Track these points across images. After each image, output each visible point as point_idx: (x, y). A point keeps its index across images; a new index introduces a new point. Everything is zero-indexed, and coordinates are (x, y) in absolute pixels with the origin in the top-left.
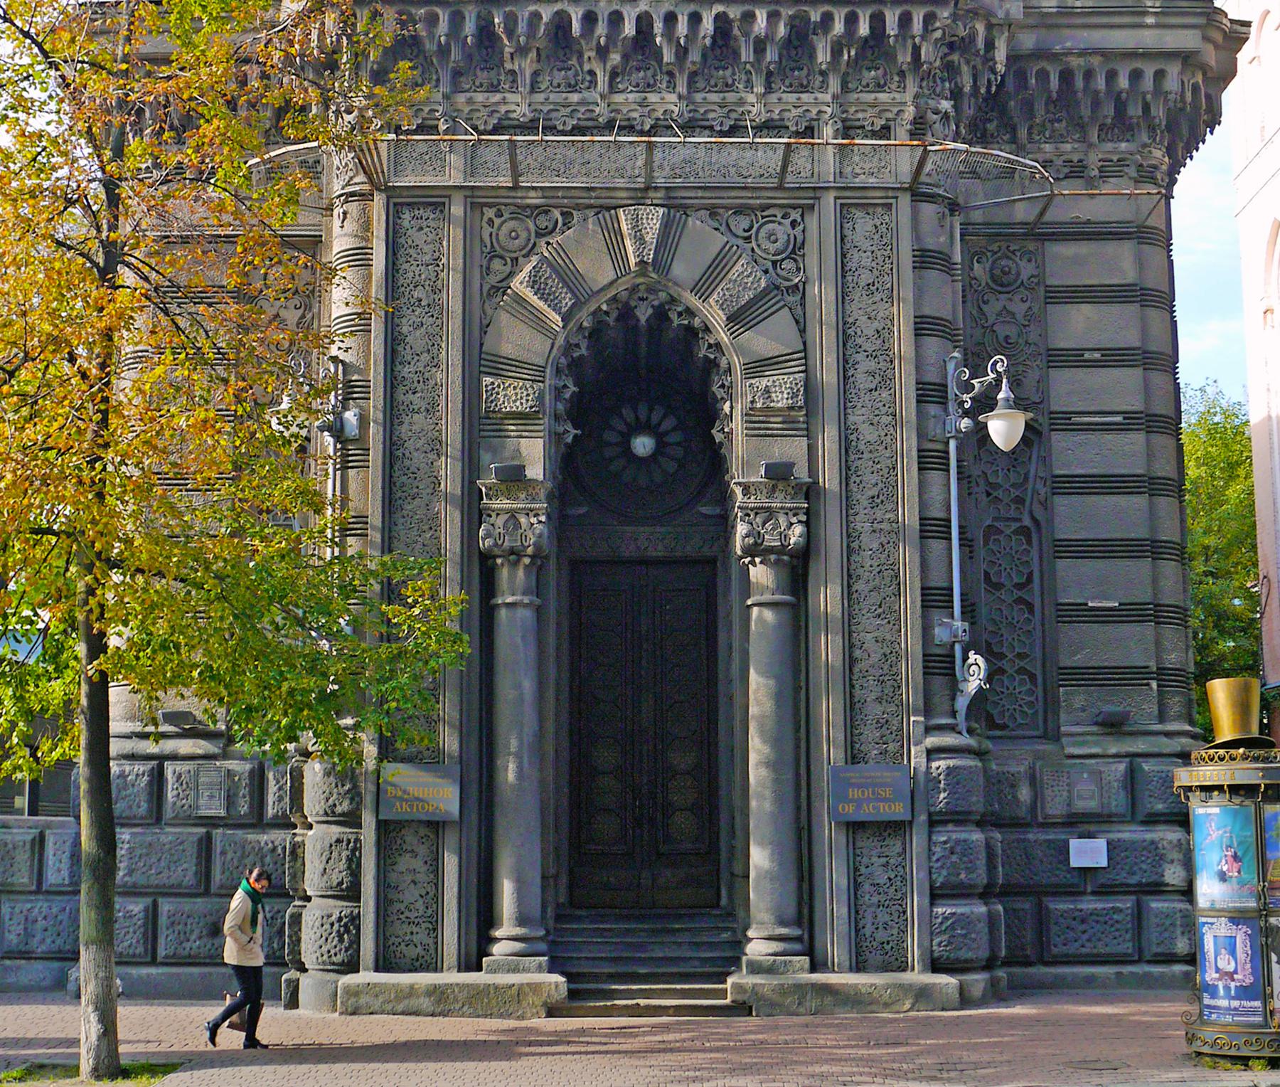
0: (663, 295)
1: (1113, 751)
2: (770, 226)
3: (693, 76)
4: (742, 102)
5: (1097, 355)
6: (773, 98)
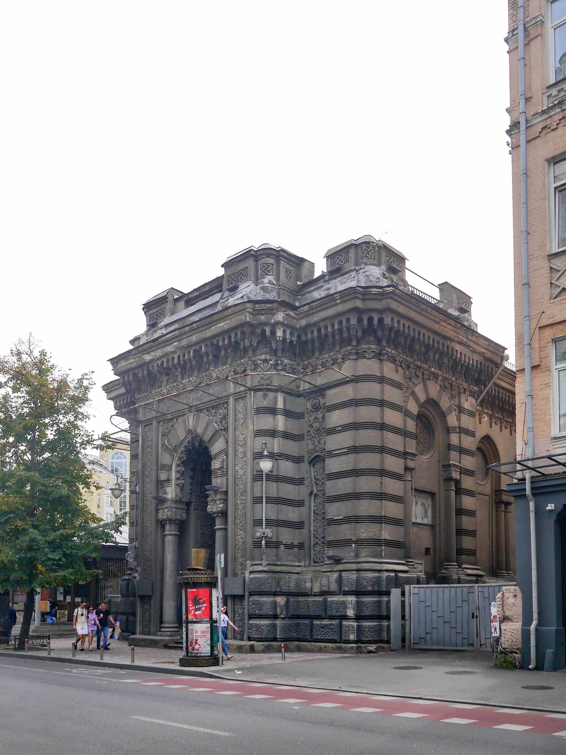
6: (216, 370)
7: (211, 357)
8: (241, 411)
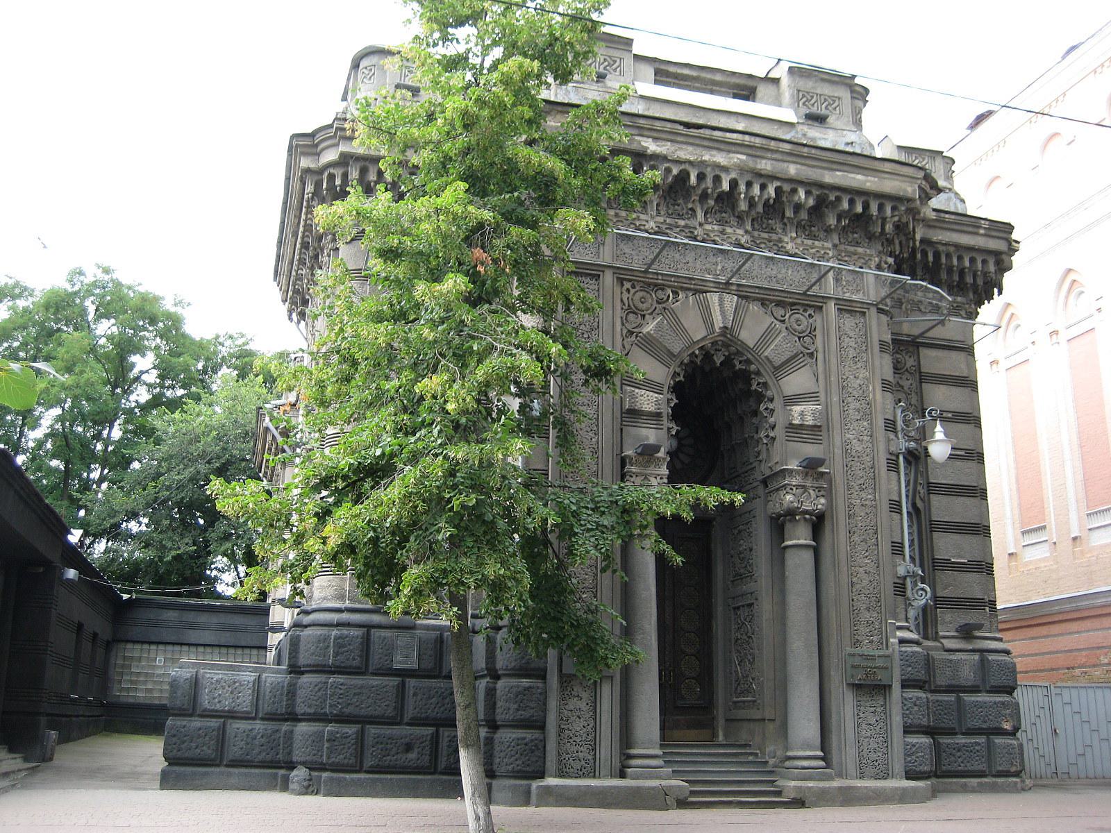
1: (971, 647)
2: (797, 315)
3: (753, 220)
4: (780, 241)
5: (950, 415)
6: (799, 241)
7: (804, 215)
8: (852, 334)
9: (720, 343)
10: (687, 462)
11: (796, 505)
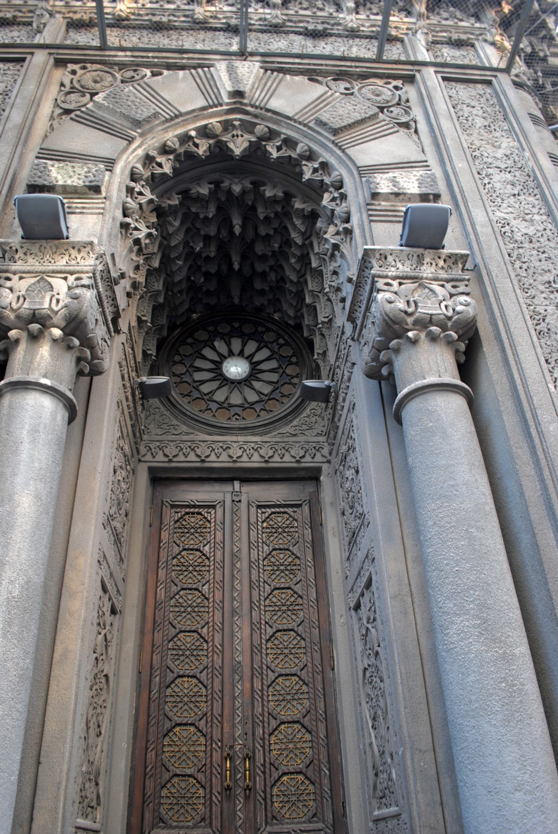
0: (260, 129)
9: (237, 123)
10: (266, 392)
11: (401, 305)
